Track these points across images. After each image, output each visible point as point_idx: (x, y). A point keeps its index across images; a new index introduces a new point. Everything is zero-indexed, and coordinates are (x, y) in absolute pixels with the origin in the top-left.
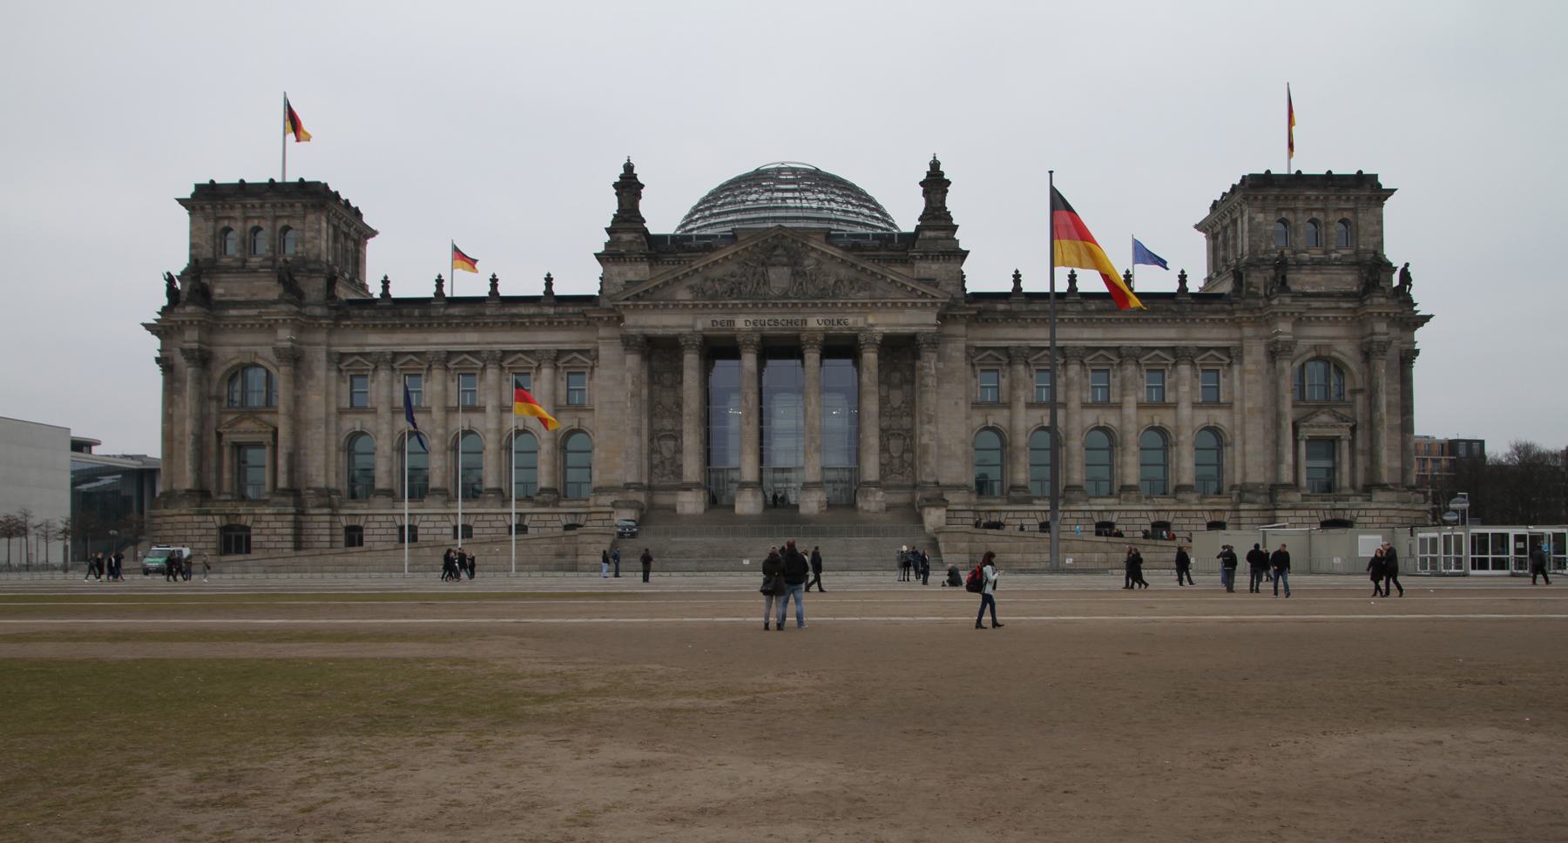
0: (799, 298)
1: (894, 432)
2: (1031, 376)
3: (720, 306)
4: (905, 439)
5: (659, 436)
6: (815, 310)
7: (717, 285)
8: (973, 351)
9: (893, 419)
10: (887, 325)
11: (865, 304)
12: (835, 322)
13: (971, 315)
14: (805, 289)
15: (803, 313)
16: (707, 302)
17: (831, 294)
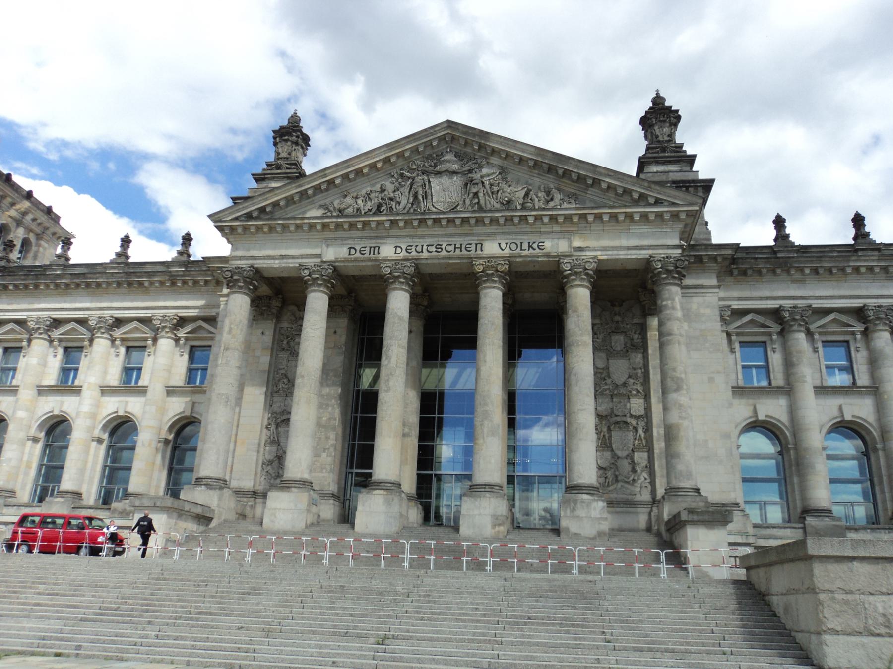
0: (474, 212)
1: (618, 419)
2: (815, 350)
3: (360, 226)
4: (636, 429)
5: (279, 420)
6: (493, 229)
7: (360, 201)
8: (729, 313)
9: (614, 400)
10: (604, 249)
11: (568, 218)
12: (525, 246)
13: (725, 258)
14: (482, 202)
15: (479, 235)
16: (340, 220)
17: (519, 207)
